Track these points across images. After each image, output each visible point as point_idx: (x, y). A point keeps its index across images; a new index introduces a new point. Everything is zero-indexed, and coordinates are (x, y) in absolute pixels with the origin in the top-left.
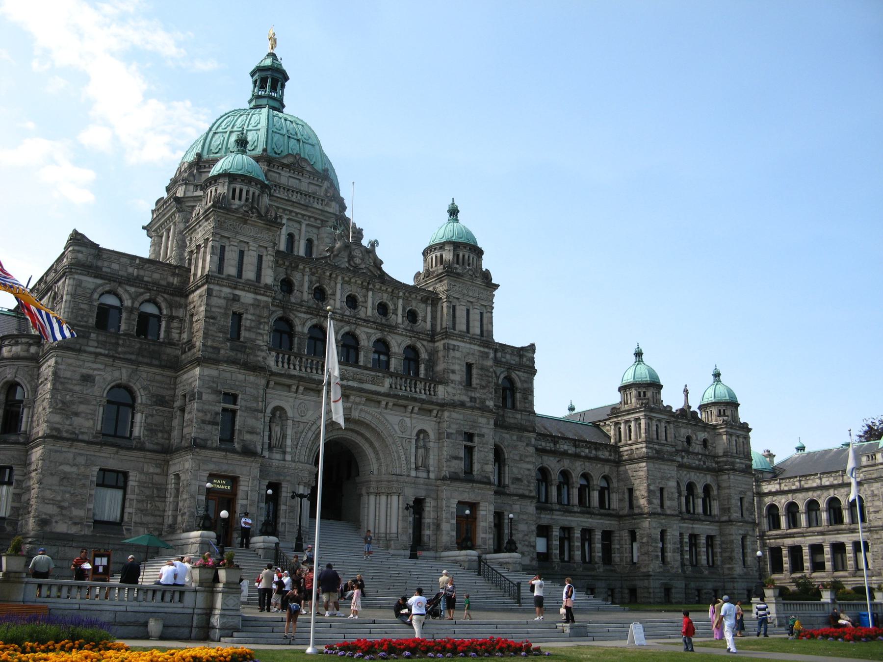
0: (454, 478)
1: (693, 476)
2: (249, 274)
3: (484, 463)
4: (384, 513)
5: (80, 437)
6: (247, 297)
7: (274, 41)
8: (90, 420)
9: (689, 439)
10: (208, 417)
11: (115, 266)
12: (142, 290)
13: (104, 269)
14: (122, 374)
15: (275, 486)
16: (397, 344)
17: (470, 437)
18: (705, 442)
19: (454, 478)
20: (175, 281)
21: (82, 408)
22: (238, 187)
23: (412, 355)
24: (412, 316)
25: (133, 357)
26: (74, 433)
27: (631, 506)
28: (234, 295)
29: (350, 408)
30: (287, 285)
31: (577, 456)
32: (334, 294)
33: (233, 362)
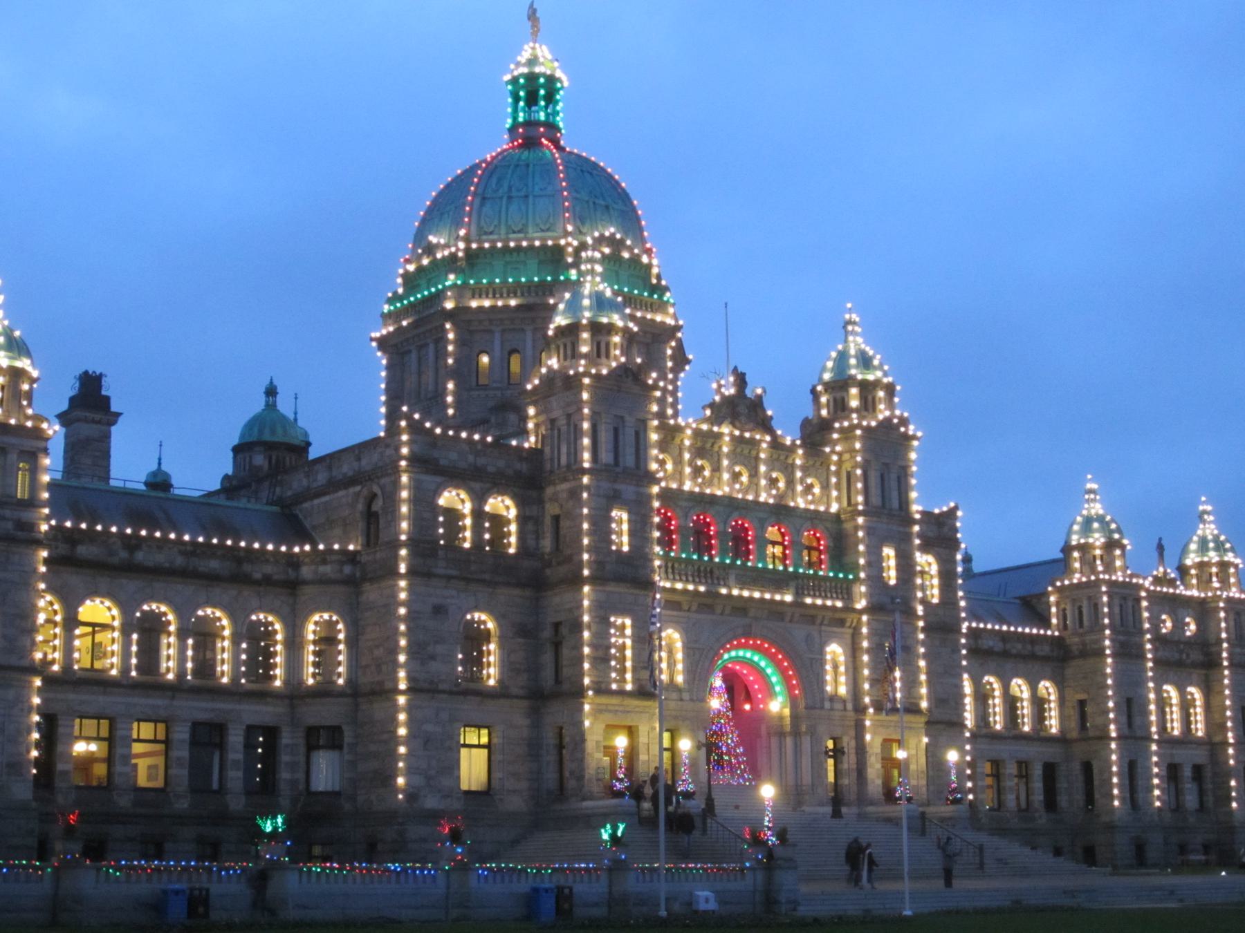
2: (629, 461)
5: (441, 687)
6: (628, 490)
10: (600, 653)
11: (454, 456)
12: (488, 485)
13: (442, 462)
20: (524, 467)
21: (439, 649)
22: (603, 339)
25: (487, 577)
26: (432, 682)
27: (1083, 727)
28: (615, 491)
29: (750, 626)
32: (717, 469)
33: (620, 579)
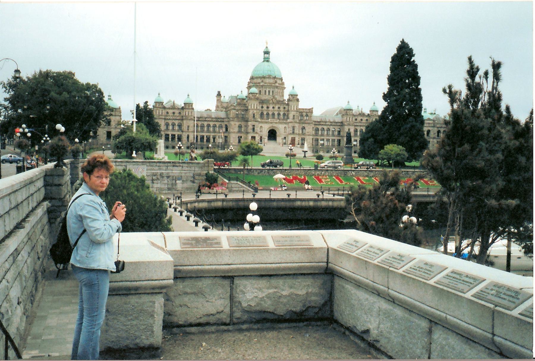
0: (290, 134)
1: (362, 128)
2: (255, 108)
3: (296, 131)
4: (279, 139)
6: (255, 111)
7: (267, 43)
8: (236, 130)
9: (362, 120)
14: (240, 123)
15: (261, 137)
16: (282, 113)
17: (294, 127)
18: (367, 120)
19: (290, 134)
23: (284, 114)
24: (285, 108)
30: (262, 107)
31: (331, 125)
